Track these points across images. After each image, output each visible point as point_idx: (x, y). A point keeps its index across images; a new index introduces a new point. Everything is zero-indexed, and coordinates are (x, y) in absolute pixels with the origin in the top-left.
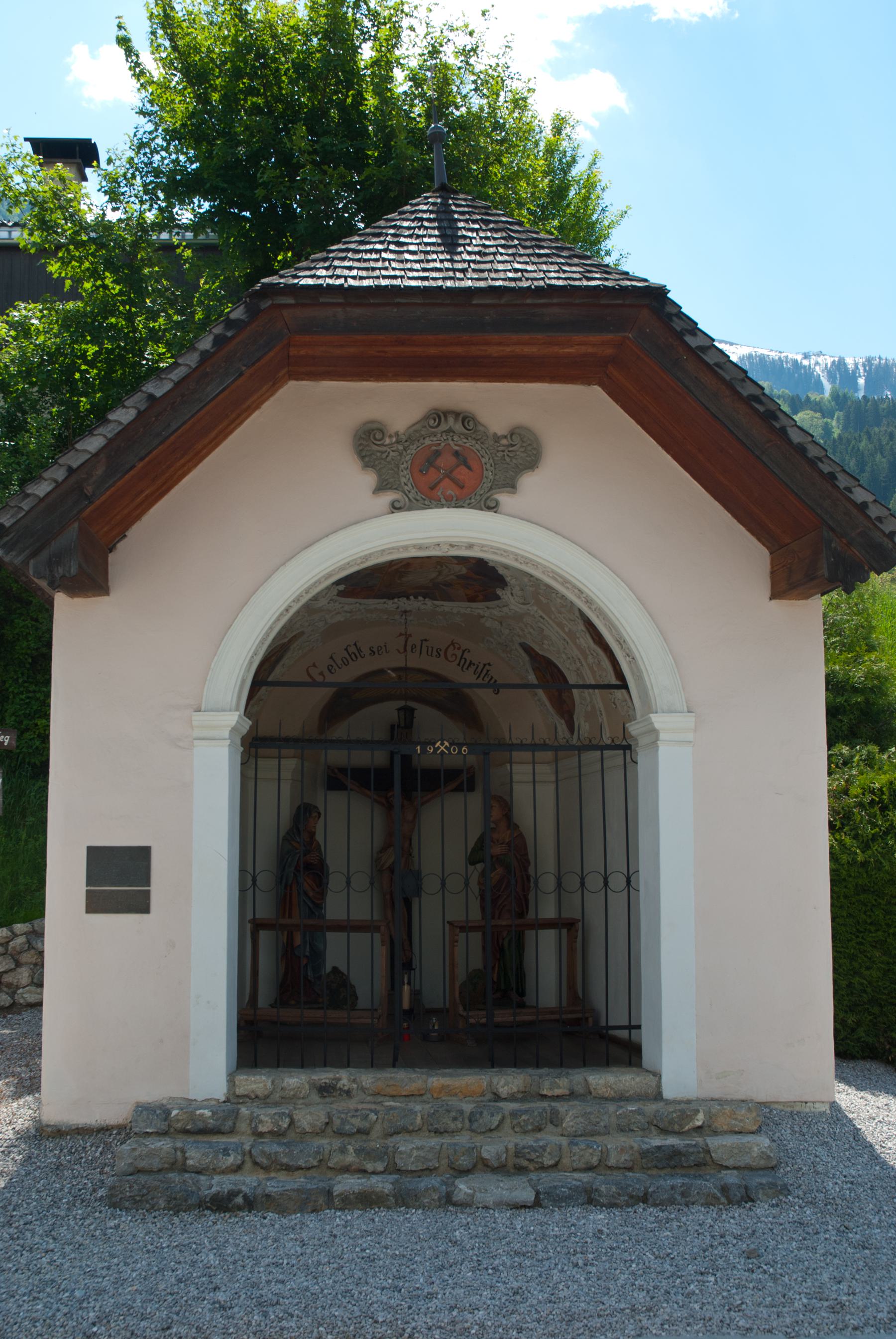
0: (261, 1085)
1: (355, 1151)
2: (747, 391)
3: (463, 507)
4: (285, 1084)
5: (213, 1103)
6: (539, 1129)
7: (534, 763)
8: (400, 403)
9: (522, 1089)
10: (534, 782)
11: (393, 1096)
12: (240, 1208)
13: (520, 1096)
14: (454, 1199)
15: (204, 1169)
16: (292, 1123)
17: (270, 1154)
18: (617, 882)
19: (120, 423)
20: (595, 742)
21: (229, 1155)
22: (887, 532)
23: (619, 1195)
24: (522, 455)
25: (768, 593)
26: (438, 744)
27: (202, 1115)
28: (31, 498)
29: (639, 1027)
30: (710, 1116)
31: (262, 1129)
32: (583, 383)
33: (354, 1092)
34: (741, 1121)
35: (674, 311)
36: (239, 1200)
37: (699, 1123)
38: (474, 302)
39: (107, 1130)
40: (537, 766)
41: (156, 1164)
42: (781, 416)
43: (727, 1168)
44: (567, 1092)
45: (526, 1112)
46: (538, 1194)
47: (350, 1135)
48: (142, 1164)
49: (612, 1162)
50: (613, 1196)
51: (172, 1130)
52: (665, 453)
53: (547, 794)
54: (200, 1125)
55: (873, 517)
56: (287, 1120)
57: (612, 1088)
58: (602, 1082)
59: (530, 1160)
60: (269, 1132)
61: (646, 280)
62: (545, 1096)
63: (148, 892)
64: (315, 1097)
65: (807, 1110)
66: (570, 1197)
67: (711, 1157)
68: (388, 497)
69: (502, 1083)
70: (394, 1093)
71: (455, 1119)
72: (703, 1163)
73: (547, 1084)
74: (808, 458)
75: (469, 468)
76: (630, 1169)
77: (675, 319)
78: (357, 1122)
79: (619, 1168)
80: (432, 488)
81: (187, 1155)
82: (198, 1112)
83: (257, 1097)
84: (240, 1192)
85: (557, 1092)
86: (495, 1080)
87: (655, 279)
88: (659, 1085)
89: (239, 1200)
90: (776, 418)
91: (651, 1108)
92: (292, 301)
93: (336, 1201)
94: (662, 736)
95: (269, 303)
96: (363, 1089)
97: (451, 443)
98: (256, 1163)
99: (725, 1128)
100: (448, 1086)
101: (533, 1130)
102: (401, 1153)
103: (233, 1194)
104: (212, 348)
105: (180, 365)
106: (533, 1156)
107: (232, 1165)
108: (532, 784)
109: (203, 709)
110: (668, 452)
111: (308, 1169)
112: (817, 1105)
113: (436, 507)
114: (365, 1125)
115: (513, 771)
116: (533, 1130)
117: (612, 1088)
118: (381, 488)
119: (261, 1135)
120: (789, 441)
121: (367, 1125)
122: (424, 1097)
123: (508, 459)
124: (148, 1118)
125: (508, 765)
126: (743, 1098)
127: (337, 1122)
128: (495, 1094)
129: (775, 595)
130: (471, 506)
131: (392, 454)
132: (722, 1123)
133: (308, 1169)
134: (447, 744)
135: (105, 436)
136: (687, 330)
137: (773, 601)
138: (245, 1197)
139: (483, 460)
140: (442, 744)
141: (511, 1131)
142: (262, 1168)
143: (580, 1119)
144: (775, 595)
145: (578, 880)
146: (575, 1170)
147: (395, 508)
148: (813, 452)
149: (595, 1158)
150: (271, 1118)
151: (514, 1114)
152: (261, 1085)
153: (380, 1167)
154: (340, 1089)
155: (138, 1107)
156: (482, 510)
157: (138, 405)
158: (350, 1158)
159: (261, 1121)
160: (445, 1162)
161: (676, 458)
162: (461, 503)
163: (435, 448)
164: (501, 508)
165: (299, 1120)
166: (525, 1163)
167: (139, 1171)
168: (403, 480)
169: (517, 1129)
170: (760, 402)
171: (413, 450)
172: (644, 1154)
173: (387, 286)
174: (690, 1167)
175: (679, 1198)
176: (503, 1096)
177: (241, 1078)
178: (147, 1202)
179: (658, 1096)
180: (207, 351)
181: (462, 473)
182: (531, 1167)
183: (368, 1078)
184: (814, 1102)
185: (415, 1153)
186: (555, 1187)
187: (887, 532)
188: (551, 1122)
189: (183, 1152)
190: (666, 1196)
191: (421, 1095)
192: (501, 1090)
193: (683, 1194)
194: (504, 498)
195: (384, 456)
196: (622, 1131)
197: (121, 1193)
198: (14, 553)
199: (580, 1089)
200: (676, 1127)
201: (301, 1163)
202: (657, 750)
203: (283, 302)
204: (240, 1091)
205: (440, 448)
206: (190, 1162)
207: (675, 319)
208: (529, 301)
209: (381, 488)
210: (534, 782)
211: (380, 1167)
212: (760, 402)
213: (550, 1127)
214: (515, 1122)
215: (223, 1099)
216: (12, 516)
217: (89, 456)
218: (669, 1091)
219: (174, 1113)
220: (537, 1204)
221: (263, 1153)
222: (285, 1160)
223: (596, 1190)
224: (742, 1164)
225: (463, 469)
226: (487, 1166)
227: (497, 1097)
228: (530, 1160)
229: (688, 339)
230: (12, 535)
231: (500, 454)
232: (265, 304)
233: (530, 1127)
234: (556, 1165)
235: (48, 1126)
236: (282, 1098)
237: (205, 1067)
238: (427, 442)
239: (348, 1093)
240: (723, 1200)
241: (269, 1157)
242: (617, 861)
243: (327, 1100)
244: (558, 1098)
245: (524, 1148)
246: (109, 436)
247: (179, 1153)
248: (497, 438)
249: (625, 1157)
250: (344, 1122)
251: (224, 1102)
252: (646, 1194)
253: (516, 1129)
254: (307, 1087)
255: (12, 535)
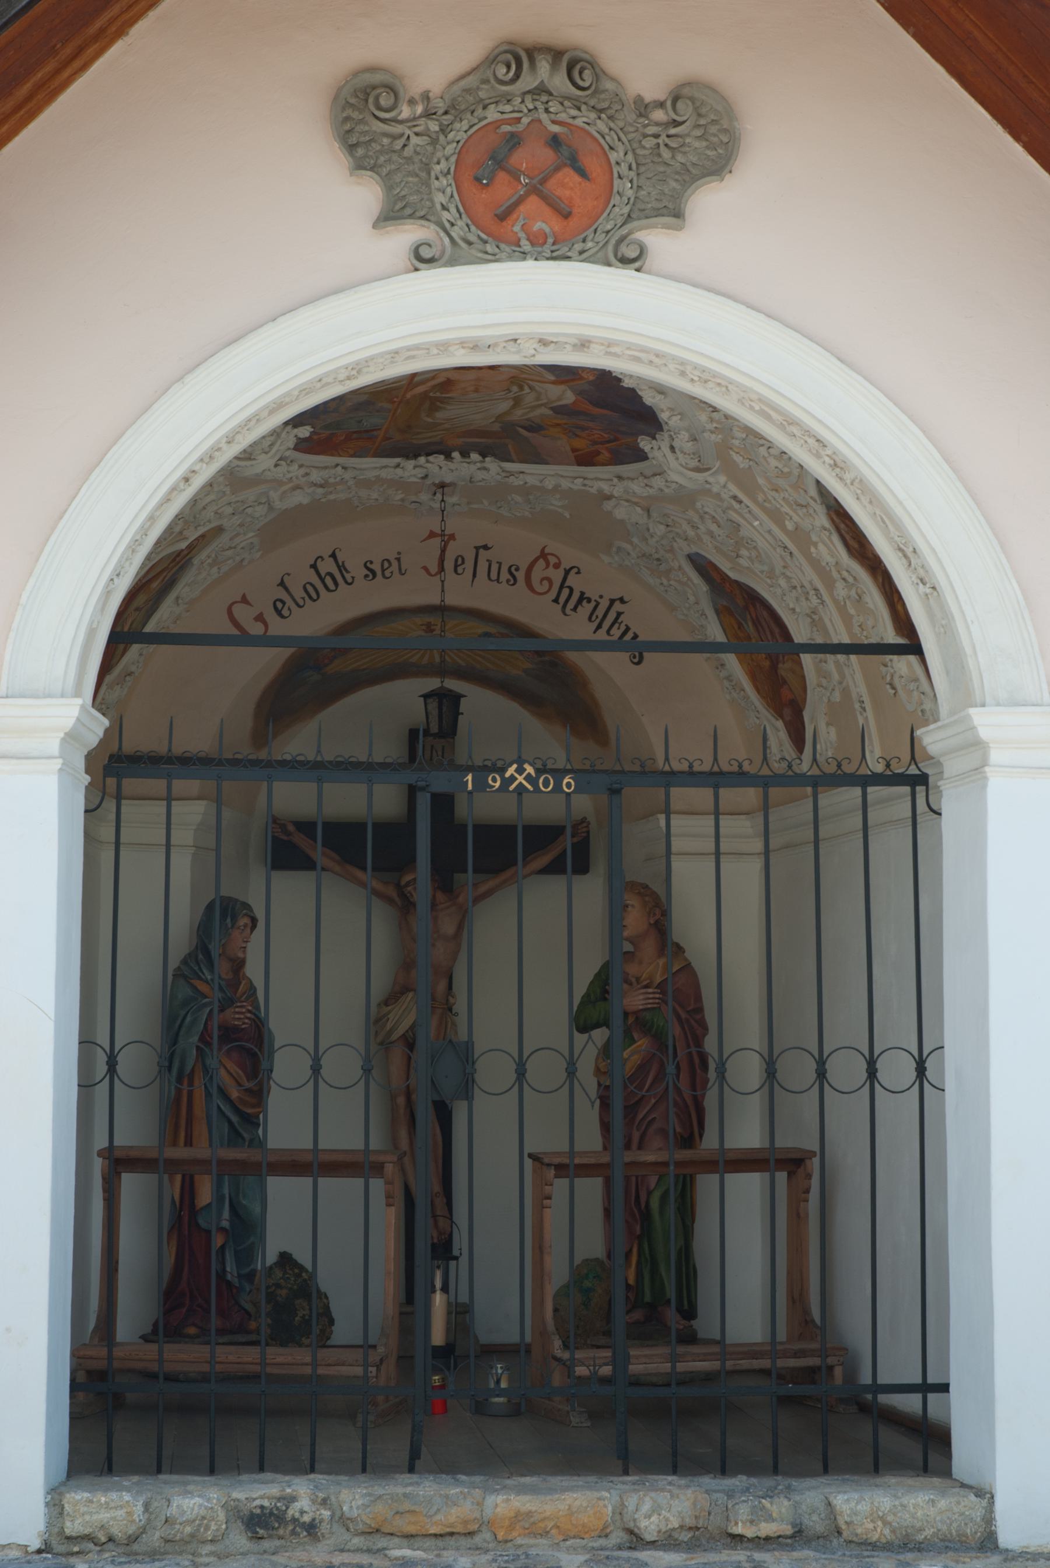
0: (120, 1513)
3: (567, 258)
4: (173, 1511)
5: (15, 1554)
7: (717, 813)
9: (689, 1522)
11: (409, 1537)
13: (685, 1536)
18: (897, 1070)
20: (848, 768)
24: (697, 144)
26: (511, 771)
29: (945, 1388)
33: (324, 1528)
40: (724, 821)
44: (788, 1530)
52: (1009, 139)
53: (744, 879)
57: (886, 1523)
58: (864, 1507)
62: (738, 1538)
64: (239, 1539)
69: (646, 1507)
70: (411, 1529)
73: (743, 1511)
75: (582, 173)
83: (111, 1539)
85: (767, 1529)
86: (631, 1501)
88: (989, 1519)
96: (344, 1521)
97: (544, 117)
100: (529, 1514)
110: (1017, 138)
113: (510, 258)
117: (886, 1523)
118: (391, 214)
122: (478, 1539)
123: (666, 154)
125: (662, 819)
128: (631, 1532)
130: (584, 256)
131: (415, 140)
134: (529, 769)
139: (613, 156)
140: (520, 770)
147: (422, 258)
152: (120, 1513)
154: (294, 1520)
156: (609, 265)
162: (564, 250)
168: (440, 198)
171: (460, 132)
176: (649, 1538)
177: (76, 1498)
181: (566, 184)
183: (355, 1497)
191: (471, 1534)
192: (643, 1523)
194: (656, 239)
195: (398, 144)
199: (816, 1523)
202: (984, 787)
204: (73, 1527)
205: (520, 127)
209: (391, 214)
210: (718, 854)
215: (36, 1544)
225: (568, 176)
227: (636, 1540)
231: (650, 142)
236: (167, 1541)
238: (492, 114)
239: (312, 1529)
242: (896, 1029)
243: (266, 1544)
248: (643, 108)
251: (39, 1552)
254: (222, 1516)
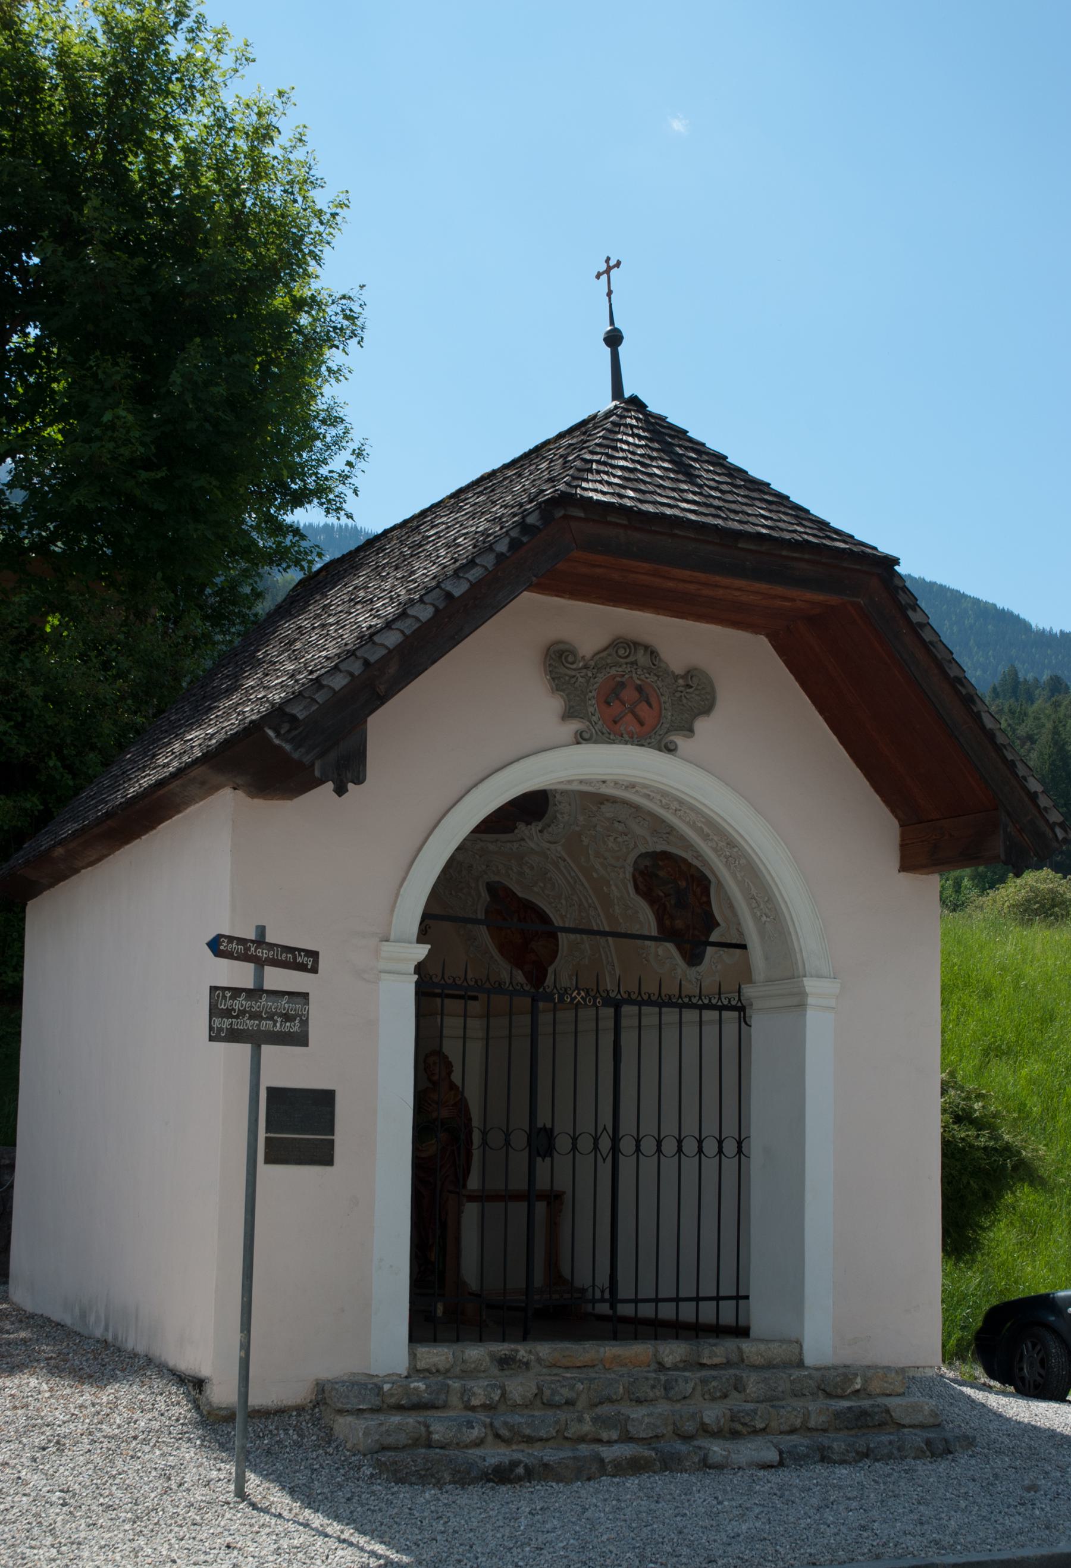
0: (443, 1358)
1: (592, 1419)
2: (953, 672)
3: (642, 745)
4: (466, 1357)
5: (395, 1378)
6: (725, 1396)
7: (465, 1016)
8: (590, 625)
9: (684, 1358)
10: (464, 1037)
11: (567, 1368)
12: (519, 1479)
13: (681, 1365)
14: (710, 1461)
15: (447, 1444)
16: (503, 1395)
17: (513, 1426)
18: (730, 1147)
19: (417, 619)
20: (653, 998)
21: (473, 1428)
22: (1051, 821)
23: (847, 1451)
24: (697, 698)
25: (897, 866)
26: (575, 994)
27: (416, 1389)
28: (325, 690)
29: (747, 1297)
30: (866, 1380)
31: (475, 1402)
32: (752, 632)
33: (532, 1364)
34: (891, 1384)
35: (901, 585)
36: (520, 1470)
37: (858, 1387)
38: (740, 545)
39: (283, 1412)
40: (469, 1020)
41: (403, 1439)
42: (977, 700)
43: (904, 1426)
44: (724, 1361)
45: (715, 1378)
46: (781, 1453)
47: (558, 1406)
48: (390, 1440)
49: (812, 1424)
50: (842, 1453)
51: (385, 1406)
52: (817, 713)
53: (475, 1049)
54: (415, 1399)
55: (1042, 806)
56: (499, 1391)
57: (762, 1356)
58: (754, 1349)
59: (745, 1424)
60: (481, 1405)
61: (875, 549)
62: (704, 1365)
63: (333, 1141)
64: (495, 1371)
65: (919, 1375)
66: (807, 1456)
67: (891, 1416)
68: (575, 726)
69: (667, 1352)
70: (569, 1364)
71: (653, 1387)
72: (885, 1421)
73: (706, 1352)
74: (996, 743)
75: (650, 705)
76: (825, 1430)
77: (900, 592)
78: (566, 1393)
79: (817, 1430)
80: (615, 722)
81: (432, 1429)
82: (412, 1385)
83: (438, 1371)
84: (520, 1462)
85: (716, 1360)
86: (661, 1348)
87: (885, 547)
88: (801, 1353)
89: (520, 1470)
90: (974, 702)
91: (796, 1374)
92: (582, 515)
93: (609, 1468)
94: (810, 1000)
95: (562, 513)
96: (539, 1360)
97: (634, 675)
98: (497, 1436)
99: (878, 1391)
100: (619, 1356)
101: (720, 1397)
102: (633, 1420)
103: (514, 1464)
104: (509, 551)
105: (477, 565)
106: (747, 1420)
107: (477, 1438)
108: (461, 1041)
109: (392, 937)
110: (821, 713)
111: (547, 1440)
112: (927, 1370)
113: (620, 743)
114: (570, 1395)
115: (445, 1024)
116: (720, 1397)
117: (762, 1356)
118: (568, 715)
119: (473, 1409)
120: (983, 727)
121: (575, 1395)
122: (596, 1369)
123: (684, 701)
124: (360, 1393)
125: (439, 1017)
126: (869, 1363)
127: (547, 1393)
128: (659, 1363)
129: (906, 866)
130: (650, 745)
131: (580, 679)
132: (875, 1387)
133: (547, 1440)
134: (583, 994)
135: (402, 632)
136: (910, 605)
137: (903, 874)
138: (526, 1467)
139: (663, 699)
140: (579, 994)
141: (701, 1399)
142: (503, 1441)
143: (761, 1385)
144: (906, 866)
145: (664, 1148)
146: (781, 1433)
147: (581, 738)
148: (1001, 739)
149: (799, 1421)
150: (484, 1390)
151: (704, 1381)
152: (443, 1358)
153: (614, 1435)
154: (520, 1360)
155: (317, 1384)
156: (660, 750)
157: (436, 603)
158: (587, 1427)
159: (474, 1394)
160: (670, 1428)
161: (827, 720)
162: (643, 742)
163: (618, 679)
164: (680, 751)
165: (511, 1392)
166: (739, 1427)
167: (384, 1448)
168: (591, 709)
169: (706, 1397)
170: (963, 685)
171: (601, 678)
172: (838, 1415)
173: (670, 516)
174: (874, 1426)
175: (895, 1452)
176: (668, 1366)
177: (422, 1350)
178: (432, 1476)
179: (801, 1364)
180: (502, 554)
181: (643, 709)
182: (744, 1431)
183: (545, 1350)
184: (924, 1367)
185: (646, 1420)
186: (795, 1446)
187: (1051, 821)
188: (736, 1389)
189: (427, 1426)
190: (886, 1451)
191: (594, 1366)
192: (666, 1359)
193: (899, 1449)
194: (679, 740)
195: (574, 680)
196: (796, 1396)
197: (406, 1468)
198: (303, 750)
199: (734, 1358)
200: (839, 1391)
201: (543, 1434)
202: (804, 1015)
203: (574, 514)
204: (421, 1365)
205: (624, 679)
206: (436, 1437)
207: (900, 592)
208: (784, 553)
209: (568, 715)
210: (464, 1037)
211: (614, 1435)
212: (963, 685)
213: (735, 1394)
214: (706, 1389)
215: (405, 1374)
216: (305, 708)
217: (384, 652)
218: (810, 1360)
219: (386, 1387)
220: (781, 1464)
221: (505, 1423)
222: (528, 1431)
223: (829, 1447)
224: (917, 1423)
225: (644, 705)
226: (706, 1431)
227: (661, 1367)
228: (745, 1424)
229: (910, 613)
230: (301, 729)
231: (678, 695)
232: (559, 513)
233: (718, 1394)
234: (764, 1430)
235: (220, 1409)
236: (463, 1371)
237: (384, 1341)
238: (613, 671)
239: (527, 1364)
240: (928, 1453)
241: (511, 1428)
242: (730, 1129)
243: (507, 1373)
244: (715, 1367)
245: (739, 1412)
246: (408, 632)
247: (423, 1428)
248: (676, 677)
249: (822, 1418)
250: (554, 1392)
251: (406, 1377)
252: (868, 1448)
253: (706, 1397)
254: (488, 1359)
255: (301, 729)
